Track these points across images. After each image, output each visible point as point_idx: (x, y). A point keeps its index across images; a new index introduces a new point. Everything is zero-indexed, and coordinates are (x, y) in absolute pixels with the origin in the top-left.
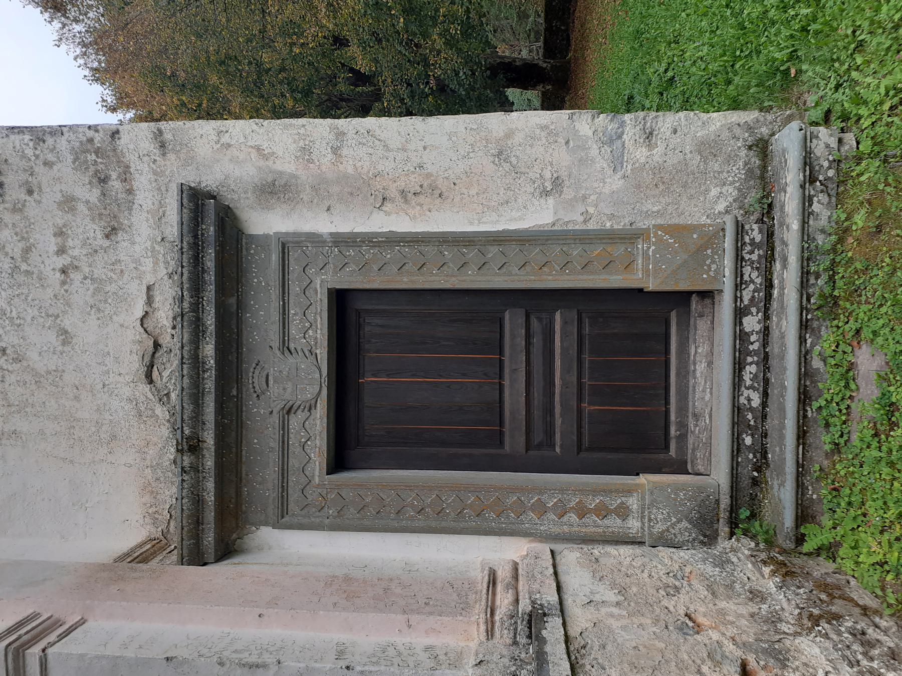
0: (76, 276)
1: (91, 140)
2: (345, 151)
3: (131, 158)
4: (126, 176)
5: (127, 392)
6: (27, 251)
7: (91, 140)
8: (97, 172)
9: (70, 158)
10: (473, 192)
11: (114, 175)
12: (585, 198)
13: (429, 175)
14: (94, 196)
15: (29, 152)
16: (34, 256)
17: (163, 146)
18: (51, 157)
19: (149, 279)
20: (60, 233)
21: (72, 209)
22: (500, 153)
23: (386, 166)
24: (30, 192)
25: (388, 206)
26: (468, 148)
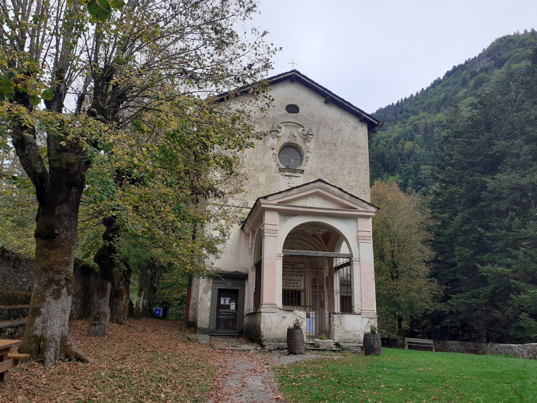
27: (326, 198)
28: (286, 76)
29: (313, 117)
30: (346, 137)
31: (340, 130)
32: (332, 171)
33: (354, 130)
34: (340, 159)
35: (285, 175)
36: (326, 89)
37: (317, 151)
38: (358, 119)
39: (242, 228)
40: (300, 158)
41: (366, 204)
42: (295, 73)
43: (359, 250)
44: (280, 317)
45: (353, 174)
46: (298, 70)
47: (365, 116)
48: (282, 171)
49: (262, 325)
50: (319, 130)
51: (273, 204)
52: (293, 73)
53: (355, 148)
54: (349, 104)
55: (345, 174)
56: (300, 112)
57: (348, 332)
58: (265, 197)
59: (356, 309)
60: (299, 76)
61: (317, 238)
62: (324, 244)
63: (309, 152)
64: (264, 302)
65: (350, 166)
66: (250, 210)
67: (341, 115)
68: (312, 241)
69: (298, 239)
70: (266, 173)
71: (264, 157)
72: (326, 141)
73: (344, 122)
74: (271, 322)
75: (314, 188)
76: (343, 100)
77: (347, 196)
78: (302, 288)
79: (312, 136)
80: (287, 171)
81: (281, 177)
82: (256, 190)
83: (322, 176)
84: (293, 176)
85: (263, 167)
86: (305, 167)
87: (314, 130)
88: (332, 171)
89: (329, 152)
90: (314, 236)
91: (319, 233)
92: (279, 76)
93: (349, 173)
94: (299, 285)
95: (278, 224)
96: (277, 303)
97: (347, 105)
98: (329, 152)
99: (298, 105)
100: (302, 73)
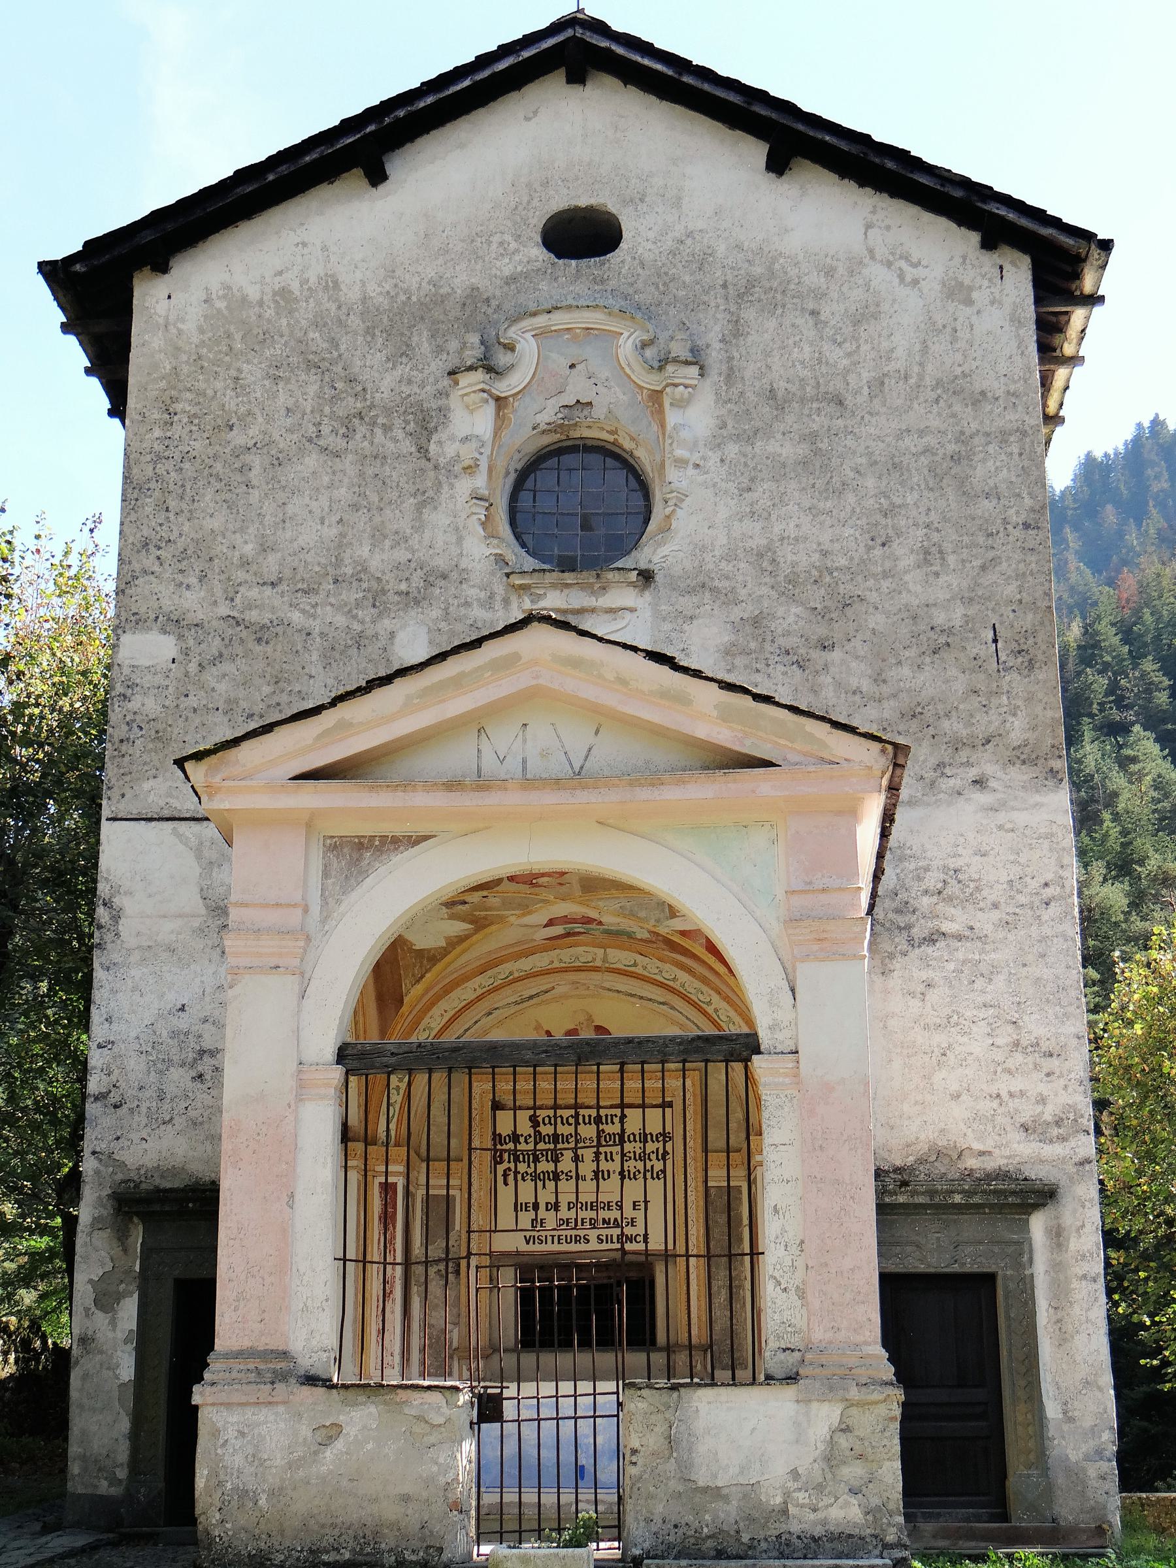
0: (995, 1105)
1: (1082, 1116)
2: (1084, 1282)
3: (1072, 1143)
4: (1063, 1139)
5: (923, 1137)
6: (1009, 1072)
7: (1082, 1116)
8: (1062, 1120)
9: (1070, 1102)
10: (1064, 1366)
11: (1061, 1131)
12: (1063, 1438)
13: (1073, 1337)
14: (1048, 1117)
15: (1072, 1075)
16: (1006, 1076)
17: (1081, 1164)
18: (1070, 1090)
19: (997, 1152)
20: (1022, 1093)
21: (1038, 1102)
22: (1088, 1383)
23: (1077, 1310)
24: (1048, 1075)
25: (1051, 1311)
26: (1090, 1362)
28: (526, 54)
29: (702, 261)
30: (900, 352)
32: (825, 554)
33: (951, 306)
34: (870, 482)
37: (732, 449)
38: (975, 237)
40: (638, 501)
41: (821, 730)
42: (579, 32)
44: (305, 1431)
45: (951, 559)
46: (594, 11)
48: (523, 587)
50: (737, 329)
52: (569, 33)
53: (957, 408)
54: (901, 155)
55: (902, 564)
57: (716, 1493)
59: (772, 1360)
60: (604, 43)
61: (694, 957)
63: (681, 463)
64: (219, 1344)
65: (934, 516)
67: (868, 226)
68: (683, 976)
69: (596, 969)
70: (436, 613)
71: (419, 527)
73: (889, 264)
74: (255, 1458)
76: (865, 139)
79: (694, 371)
80: (554, 586)
83: (765, 590)
84: (593, 610)
85: (417, 580)
86: (664, 550)
87: (712, 333)
88: (825, 554)
89: (803, 449)
92: (483, 61)
93: (928, 555)
97: (890, 165)
98: (803, 449)
100: (617, 26)
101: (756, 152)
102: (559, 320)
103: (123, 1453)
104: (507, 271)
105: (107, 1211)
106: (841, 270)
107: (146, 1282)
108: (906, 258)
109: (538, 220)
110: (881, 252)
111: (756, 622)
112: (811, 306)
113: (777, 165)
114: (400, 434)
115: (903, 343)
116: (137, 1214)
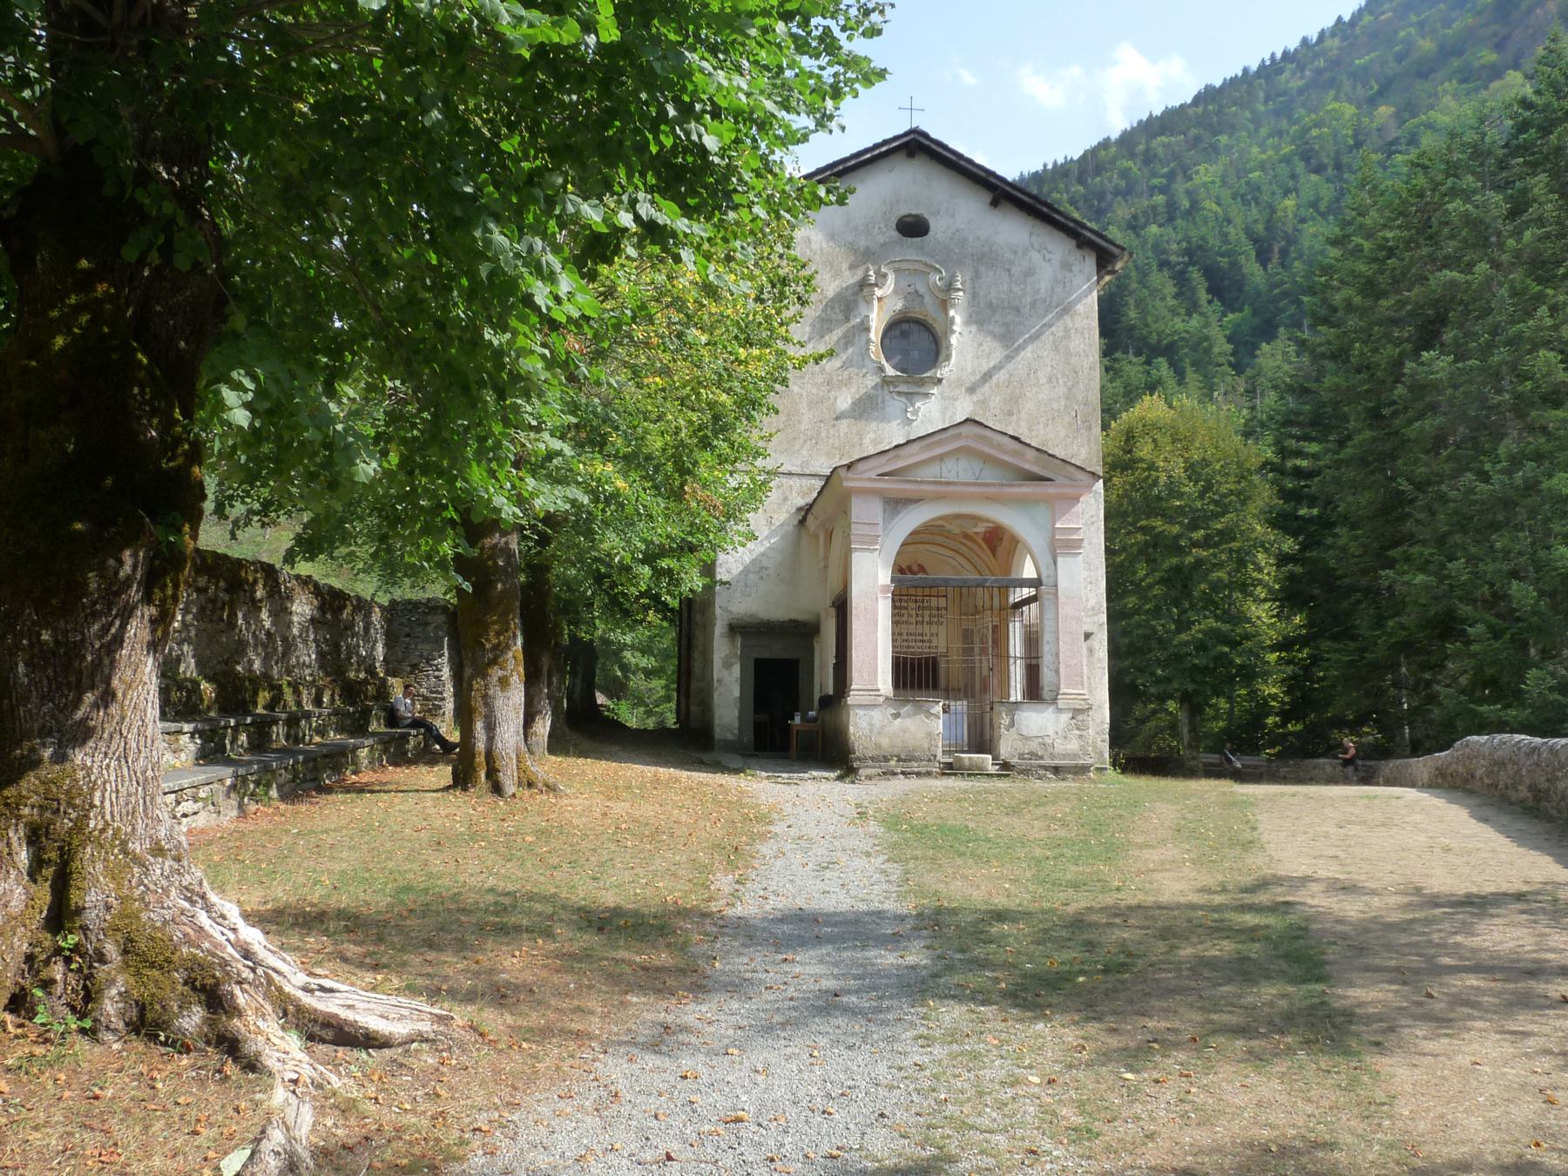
27: (987, 459)
29: (963, 243)
30: (1043, 291)
31: (1030, 273)
35: (899, 393)
36: (993, 174)
38: (1074, 243)
39: (802, 522)
42: (916, 136)
43: (1056, 569)
46: (924, 128)
47: (1089, 234)
49: (851, 729)
51: (870, 479)
52: (912, 136)
56: (931, 233)
58: (849, 466)
60: (927, 143)
61: (974, 541)
62: (988, 552)
66: (819, 484)
72: (994, 301)
74: (871, 724)
75: (958, 436)
77: (1031, 454)
78: (942, 649)
81: (888, 397)
82: (832, 432)
84: (917, 393)
90: (966, 536)
91: (976, 530)
94: (934, 644)
95: (880, 520)
96: (880, 686)
99: (926, 216)
101: (987, 197)
102: (904, 266)
103: (736, 724)
104: (882, 241)
105: (725, 630)
106: (1020, 253)
107: (743, 658)
108: (1046, 249)
109: (894, 220)
110: (1036, 246)
111: (983, 402)
112: (1007, 266)
113: (995, 204)
114: (837, 310)
115: (1044, 286)
116: (741, 633)
